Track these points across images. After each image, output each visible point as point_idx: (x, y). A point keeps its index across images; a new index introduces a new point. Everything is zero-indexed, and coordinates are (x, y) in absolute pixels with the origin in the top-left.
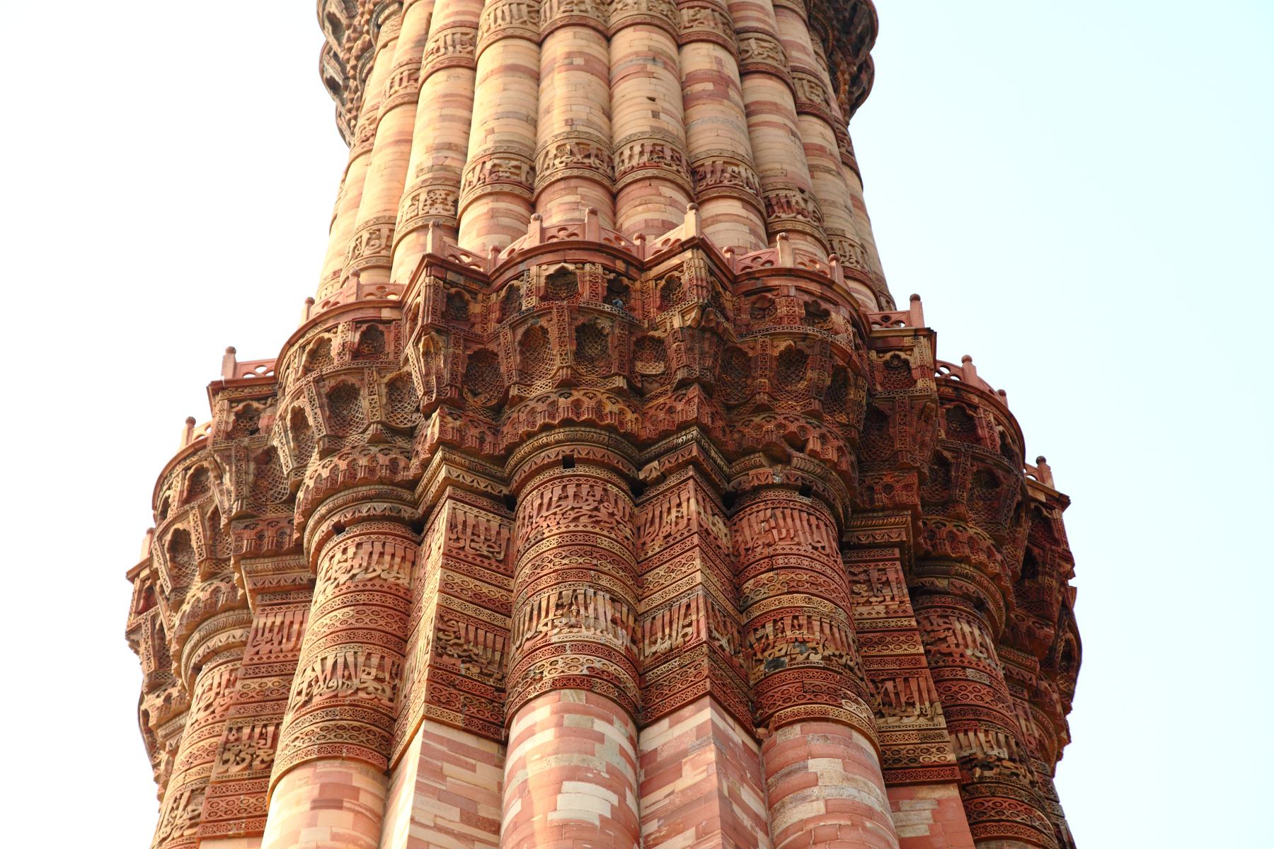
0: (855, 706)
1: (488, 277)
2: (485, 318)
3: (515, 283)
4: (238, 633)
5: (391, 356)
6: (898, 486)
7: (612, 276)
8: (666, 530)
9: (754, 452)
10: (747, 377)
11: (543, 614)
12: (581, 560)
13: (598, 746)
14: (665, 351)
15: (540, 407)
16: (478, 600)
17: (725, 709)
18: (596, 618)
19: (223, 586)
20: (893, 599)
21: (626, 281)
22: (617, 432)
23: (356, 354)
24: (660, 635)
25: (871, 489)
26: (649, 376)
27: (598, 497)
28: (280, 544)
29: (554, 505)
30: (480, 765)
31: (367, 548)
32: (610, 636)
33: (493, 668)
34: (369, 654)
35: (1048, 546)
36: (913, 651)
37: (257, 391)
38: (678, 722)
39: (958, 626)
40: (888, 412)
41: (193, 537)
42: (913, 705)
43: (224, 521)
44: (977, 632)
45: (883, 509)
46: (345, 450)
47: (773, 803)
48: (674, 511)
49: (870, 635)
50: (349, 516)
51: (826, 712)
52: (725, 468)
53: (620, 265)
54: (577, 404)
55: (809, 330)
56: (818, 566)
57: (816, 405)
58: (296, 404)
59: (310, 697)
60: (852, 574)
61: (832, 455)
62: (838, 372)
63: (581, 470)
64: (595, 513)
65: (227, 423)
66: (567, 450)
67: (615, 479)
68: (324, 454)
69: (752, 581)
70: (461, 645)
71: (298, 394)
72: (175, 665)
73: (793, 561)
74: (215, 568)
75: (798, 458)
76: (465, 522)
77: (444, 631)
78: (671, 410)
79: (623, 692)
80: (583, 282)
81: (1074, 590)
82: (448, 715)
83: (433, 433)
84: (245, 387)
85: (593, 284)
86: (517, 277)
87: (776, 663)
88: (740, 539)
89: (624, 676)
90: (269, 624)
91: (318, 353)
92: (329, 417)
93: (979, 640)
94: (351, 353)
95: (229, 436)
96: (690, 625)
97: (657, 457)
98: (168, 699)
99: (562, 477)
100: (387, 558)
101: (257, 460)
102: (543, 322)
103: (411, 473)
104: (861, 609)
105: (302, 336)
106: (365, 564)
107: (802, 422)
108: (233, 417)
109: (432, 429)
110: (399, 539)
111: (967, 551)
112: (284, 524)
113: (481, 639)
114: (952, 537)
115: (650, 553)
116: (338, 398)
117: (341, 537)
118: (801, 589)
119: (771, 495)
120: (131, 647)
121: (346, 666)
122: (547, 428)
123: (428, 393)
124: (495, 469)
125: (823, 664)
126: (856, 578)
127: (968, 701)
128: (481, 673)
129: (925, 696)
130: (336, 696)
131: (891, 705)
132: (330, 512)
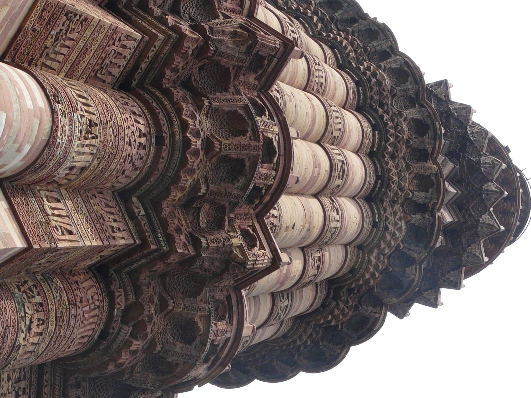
7: (263, 191)
8: (106, 217)
9: (136, 294)
10: (183, 293)
13: (17, 146)
24: (53, 205)
26: (198, 214)
29: (137, 124)
33: (43, 60)
48: (115, 225)
52: (127, 269)
53: (267, 198)
60: (24, 368)
61: (125, 357)
62: (171, 367)
66: (167, 141)
70: (66, 34)
73: (72, 322)
75: (128, 329)
78: (179, 230)
86: (270, 115)
96: (63, 234)
97: (147, 215)
103: (151, 5)
107: (149, 337)
115: (92, 201)
118: (58, 327)
125: (17, 344)
128: (46, 48)
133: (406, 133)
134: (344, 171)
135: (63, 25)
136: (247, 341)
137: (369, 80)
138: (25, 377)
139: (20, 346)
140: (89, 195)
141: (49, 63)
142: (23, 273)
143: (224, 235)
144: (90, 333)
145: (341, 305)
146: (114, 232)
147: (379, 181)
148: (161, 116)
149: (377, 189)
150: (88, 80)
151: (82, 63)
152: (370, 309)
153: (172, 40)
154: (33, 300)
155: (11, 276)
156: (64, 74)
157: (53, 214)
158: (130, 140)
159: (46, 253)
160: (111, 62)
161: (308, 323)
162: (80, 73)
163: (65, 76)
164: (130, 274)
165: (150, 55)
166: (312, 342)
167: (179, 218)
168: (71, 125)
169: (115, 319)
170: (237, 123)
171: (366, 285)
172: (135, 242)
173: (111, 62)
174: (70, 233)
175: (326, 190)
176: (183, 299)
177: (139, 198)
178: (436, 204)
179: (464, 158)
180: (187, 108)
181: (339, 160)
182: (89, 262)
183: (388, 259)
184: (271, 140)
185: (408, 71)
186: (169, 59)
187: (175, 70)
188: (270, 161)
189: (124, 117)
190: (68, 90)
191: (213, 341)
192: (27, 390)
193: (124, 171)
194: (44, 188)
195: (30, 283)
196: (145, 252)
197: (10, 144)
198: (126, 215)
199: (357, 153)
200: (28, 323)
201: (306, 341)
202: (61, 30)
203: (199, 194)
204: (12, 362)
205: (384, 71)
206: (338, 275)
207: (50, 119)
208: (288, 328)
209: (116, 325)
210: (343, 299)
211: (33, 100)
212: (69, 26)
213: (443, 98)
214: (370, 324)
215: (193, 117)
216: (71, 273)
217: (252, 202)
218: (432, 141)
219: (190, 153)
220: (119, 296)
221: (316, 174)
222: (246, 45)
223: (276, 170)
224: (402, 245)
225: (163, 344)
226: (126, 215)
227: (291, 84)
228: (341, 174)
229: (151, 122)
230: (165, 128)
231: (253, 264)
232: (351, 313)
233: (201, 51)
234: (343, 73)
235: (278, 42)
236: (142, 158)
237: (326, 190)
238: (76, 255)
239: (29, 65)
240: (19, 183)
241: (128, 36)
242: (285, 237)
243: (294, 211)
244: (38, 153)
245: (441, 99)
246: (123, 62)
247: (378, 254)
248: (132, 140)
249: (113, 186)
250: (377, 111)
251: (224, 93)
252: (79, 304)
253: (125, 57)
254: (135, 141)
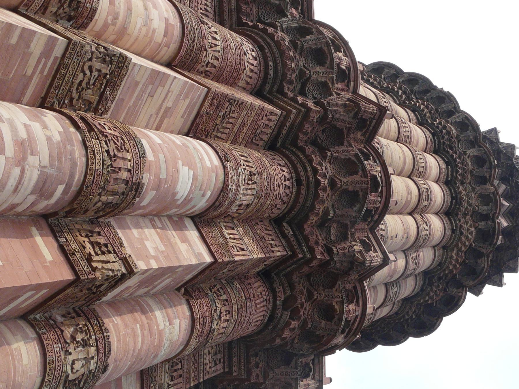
7: (373, 212)
10: (323, 286)
13: (203, 192)
20: (210, 368)
23: (338, 65)
24: (230, 232)
26: (330, 231)
30: (183, 120)
37: (306, 9)
42: (172, 380)
47: (154, 296)
48: (273, 242)
52: (284, 272)
53: (377, 216)
60: (219, 345)
61: (287, 333)
62: (320, 338)
66: (304, 182)
67: (287, 209)
70: (229, 114)
73: (249, 311)
78: (317, 243)
79: (215, 209)
86: (374, 159)
92: (311, 48)
96: (238, 251)
97: (295, 234)
100: (250, 74)
103: (286, 91)
106: (250, 61)
107: (302, 318)
112: (251, 18)
115: (256, 228)
121: (216, 45)
128: (217, 125)
130: (205, 39)
131: (172, 367)
133: (470, 166)
134: (428, 195)
135: (227, 108)
136: (371, 318)
137: (441, 131)
138: (219, 351)
139: (214, 329)
140: (254, 223)
141: (219, 135)
142: (213, 280)
143: (349, 244)
144: (261, 318)
145: (434, 289)
146: (272, 247)
147: (454, 201)
148: (298, 165)
149: (453, 207)
151: (242, 134)
152: (455, 290)
154: (221, 298)
155: (205, 282)
156: (230, 142)
157: (230, 238)
158: (279, 184)
159: (227, 265)
160: (261, 131)
161: (412, 303)
162: (241, 140)
164: (285, 275)
165: (288, 124)
166: (416, 316)
167: (316, 235)
168: (237, 175)
169: (278, 307)
170: (352, 166)
171: (450, 273)
173: (261, 131)
174: (243, 250)
175: (417, 210)
176: (324, 290)
177: (289, 223)
178: (495, 213)
179: (513, 181)
180: (316, 159)
181: (425, 188)
182: (257, 270)
183: (465, 254)
184: (375, 177)
185: (467, 123)
186: (301, 126)
187: (306, 134)
188: (376, 191)
189: (273, 168)
190: (234, 152)
191: (346, 318)
192: (222, 360)
193: (276, 205)
194: (223, 221)
195: (218, 286)
196: (295, 259)
197: (197, 192)
198: (280, 236)
199: (437, 182)
200: (219, 314)
201: (412, 316)
202: (226, 112)
203: (329, 217)
204: (210, 341)
205: (451, 124)
206: (431, 268)
207: (223, 172)
208: (399, 307)
209: (279, 311)
210: (435, 284)
211: (211, 160)
212: (231, 109)
213: (494, 140)
214: (456, 301)
215: (321, 164)
216: (245, 277)
217: (366, 220)
218: (489, 170)
219: (320, 189)
220: (280, 291)
221: (409, 199)
222: (353, 113)
223: (381, 197)
224: (474, 244)
225: (312, 322)
226: (280, 236)
227: (387, 138)
228: (427, 197)
229: (292, 170)
230: (302, 174)
232: (441, 294)
233: (323, 119)
234: (422, 128)
235: (375, 109)
236: (288, 195)
237: (417, 210)
238: (247, 265)
239: (206, 137)
240: (206, 218)
241: (272, 112)
242: (391, 244)
243: (396, 226)
244: (216, 197)
245: (492, 141)
246: (270, 131)
247: (457, 251)
248: (280, 183)
249: (270, 216)
250: (448, 152)
251: (341, 146)
252: (252, 299)
253: (271, 127)
254: (282, 184)
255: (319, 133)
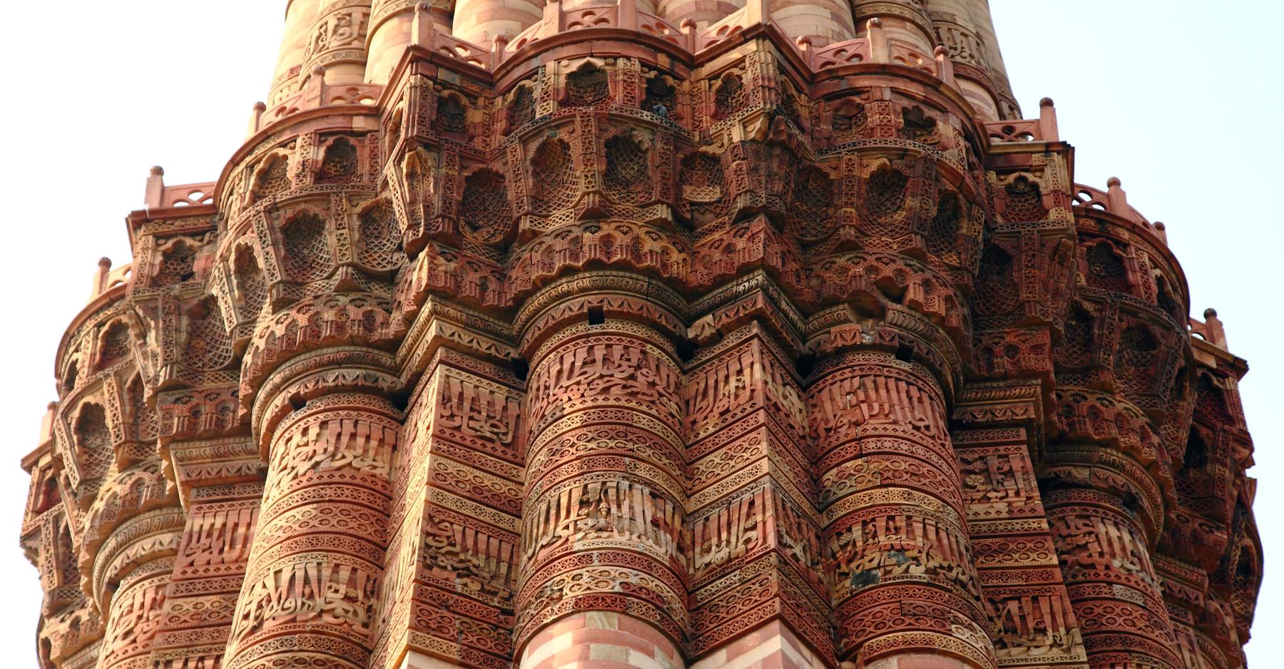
0: (968, 633)
1: (492, 76)
2: (487, 128)
3: (527, 83)
4: (166, 538)
5: (366, 178)
6: (1024, 347)
7: (652, 74)
8: (722, 404)
9: (837, 304)
11: (563, 513)
12: (612, 444)
14: (721, 171)
15: (560, 245)
16: (479, 495)
17: (800, 637)
18: (632, 519)
19: (147, 477)
20: (1017, 494)
21: (670, 81)
22: (661, 279)
23: (320, 175)
24: (714, 541)
25: (989, 350)
26: (700, 204)
27: (634, 362)
28: (220, 423)
29: (577, 372)
31: (334, 427)
32: (651, 542)
33: (498, 584)
34: (337, 566)
35: (1219, 425)
36: (1044, 562)
37: (190, 224)
38: (738, 654)
39: (1102, 529)
40: (1012, 252)
41: (108, 414)
42: (1044, 631)
43: (148, 392)
44: (1127, 537)
45: (1005, 377)
46: (306, 301)
49: (988, 541)
50: (311, 386)
51: (931, 641)
52: (800, 324)
53: (663, 61)
54: (607, 241)
55: (909, 144)
56: (920, 452)
57: (918, 242)
58: (241, 240)
59: (260, 622)
61: (938, 307)
62: (946, 200)
63: (612, 326)
64: (630, 382)
65: (152, 265)
66: (594, 300)
67: (657, 337)
68: (277, 306)
69: (835, 470)
70: (456, 554)
71: (244, 228)
72: (84, 580)
73: (888, 444)
74: (136, 454)
75: (894, 311)
76: (461, 394)
77: (434, 535)
78: (729, 249)
79: (666, 615)
80: (615, 82)
81: (1253, 482)
82: (440, 645)
83: (419, 278)
84: (176, 218)
85: (628, 84)
86: (529, 76)
87: (866, 577)
88: (819, 416)
89: (668, 593)
90: (206, 527)
91: (270, 174)
92: (285, 258)
93: (1129, 547)
94: (315, 173)
95: (155, 282)
96: (754, 528)
97: (711, 309)
98: (75, 624)
99: (588, 336)
100: (360, 441)
101: (192, 314)
102: (563, 134)
103: (392, 331)
104: (977, 507)
105: (250, 153)
106: (331, 449)
107: (900, 264)
108: (159, 258)
109: (419, 273)
110: (376, 416)
111: (1114, 432)
112: (226, 396)
113: (482, 546)
114: (1095, 414)
115: (702, 435)
116: (297, 234)
117: (301, 413)
118: (898, 481)
119: (859, 358)
120: (28, 556)
121: (307, 581)
122: (567, 271)
123: (413, 226)
124: (501, 326)
125: (926, 578)
126: (970, 467)
127: (1115, 627)
128: (482, 590)
129: (1060, 620)
130: (294, 620)
131: (1015, 632)
132: (287, 382)
141: (504, 568)
148: (557, 314)
150: (519, 460)
153: (438, 308)
163: (520, 517)
172: (756, 335)
203: (670, 219)
229: (567, 334)
231: (770, 89)
255: (480, 239)
